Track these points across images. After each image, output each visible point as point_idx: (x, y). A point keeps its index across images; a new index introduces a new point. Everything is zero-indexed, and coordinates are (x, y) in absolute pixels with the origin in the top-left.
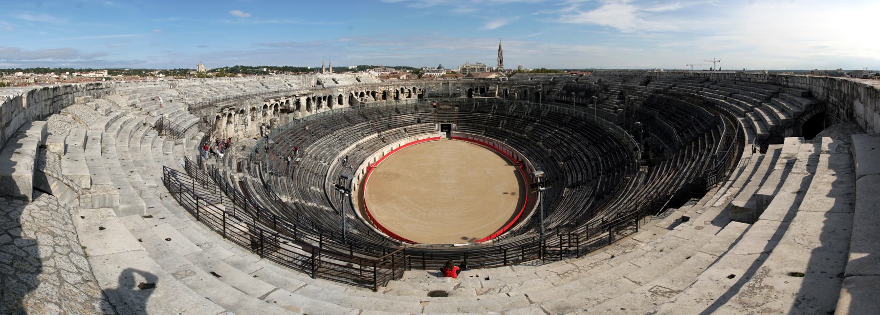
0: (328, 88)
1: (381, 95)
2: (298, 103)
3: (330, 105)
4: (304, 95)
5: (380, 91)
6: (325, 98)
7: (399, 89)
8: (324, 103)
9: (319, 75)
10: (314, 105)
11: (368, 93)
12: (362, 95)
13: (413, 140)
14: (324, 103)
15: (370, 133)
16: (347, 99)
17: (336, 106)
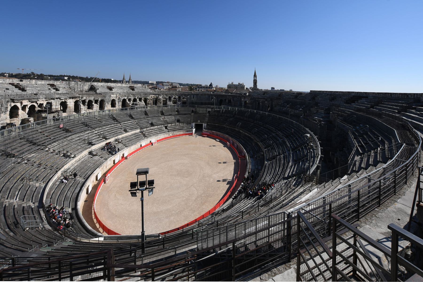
0: (100, 94)
1: (152, 102)
2: (64, 105)
3: (102, 107)
4: (73, 98)
5: (151, 97)
6: (96, 102)
7: (167, 97)
8: (96, 107)
9: (95, 84)
10: (84, 109)
11: (140, 100)
12: (135, 100)
13: (171, 135)
14: (96, 107)
15: (132, 129)
16: (121, 103)
17: (108, 107)
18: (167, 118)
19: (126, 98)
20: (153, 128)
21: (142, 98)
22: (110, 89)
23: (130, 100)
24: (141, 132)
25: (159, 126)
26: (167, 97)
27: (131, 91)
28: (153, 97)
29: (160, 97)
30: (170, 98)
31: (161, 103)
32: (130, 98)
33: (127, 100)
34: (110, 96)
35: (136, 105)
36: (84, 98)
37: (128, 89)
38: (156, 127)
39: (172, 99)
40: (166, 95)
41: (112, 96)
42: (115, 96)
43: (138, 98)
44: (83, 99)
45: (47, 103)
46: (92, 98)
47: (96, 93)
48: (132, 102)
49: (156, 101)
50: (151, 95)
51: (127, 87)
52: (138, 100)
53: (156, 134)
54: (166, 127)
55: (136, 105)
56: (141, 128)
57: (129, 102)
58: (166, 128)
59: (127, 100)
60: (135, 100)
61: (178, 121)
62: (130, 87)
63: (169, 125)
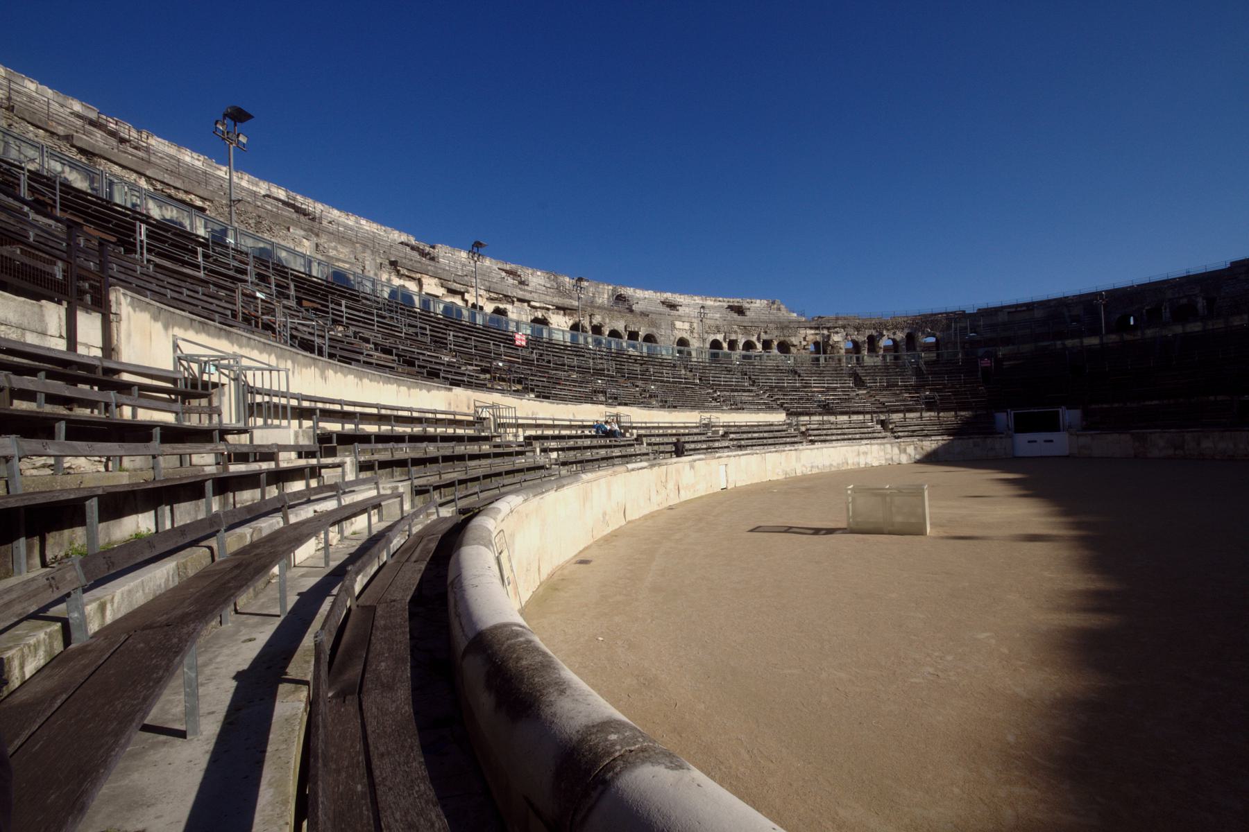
0: (644, 314)
7: (862, 338)
19: (720, 337)
20: (832, 418)
22: (673, 306)
25: (855, 417)
26: (862, 338)
27: (736, 316)
28: (810, 338)
29: (836, 338)
30: (872, 341)
32: (733, 337)
34: (673, 326)
36: (597, 320)
38: (845, 418)
40: (858, 329)
41: (678, 324)
42: (687, 326)
43: (759, 339)
44: (595, 322)
45: (498, 311)
46: (620, 326)
47: (631, 311)
50: (803, 332)
54: (883, 423)
56: (789, 414)
59: (725, 345)
60: (749, 345)
61: (930, 406)
63: (896, 417)
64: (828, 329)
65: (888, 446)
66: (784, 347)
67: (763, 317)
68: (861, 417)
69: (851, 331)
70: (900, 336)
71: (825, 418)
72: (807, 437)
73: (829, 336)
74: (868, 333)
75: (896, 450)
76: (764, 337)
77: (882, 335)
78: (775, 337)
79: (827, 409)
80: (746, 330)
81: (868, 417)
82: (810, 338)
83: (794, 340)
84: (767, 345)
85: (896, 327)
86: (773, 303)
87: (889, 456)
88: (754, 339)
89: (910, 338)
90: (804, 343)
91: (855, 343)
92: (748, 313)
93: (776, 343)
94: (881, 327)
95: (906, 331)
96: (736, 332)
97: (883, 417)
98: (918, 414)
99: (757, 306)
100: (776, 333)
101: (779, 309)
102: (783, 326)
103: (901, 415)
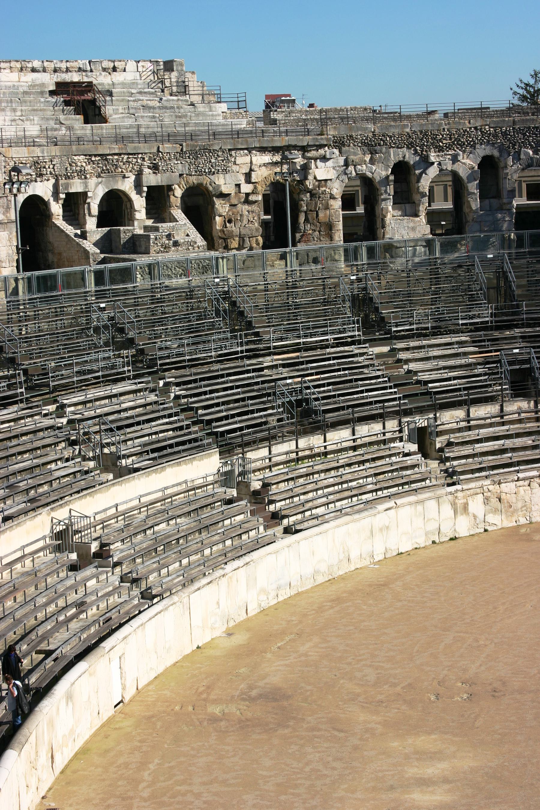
7: (380, 172)
12: (115, 209)
15: (160, 454)
18: (430, 362)
19: (43, 189)
20: (316, 441)
21: (169, 188)
23: (74, 205)
24: (226, 479)
25: (363, 430)
26: (380, 172)
29: (321, 171)
31: (330, 227)
32: (76, 187)
33: (56, 209)
35: (137, 245)
37: (51, 107)
39: (425, 184)
43: (138, 185)
48: (91, 224)
49: (283, 212)
51: (36, 90)
52: (139, 203)
53: (356, 498)
54: (422, 437)
55: (137, 245)
56: (226, 450)
57: (70, 230)
58: (424, 451)
59: (56, 209)
60: (115, 209)
62: (62, 88)
63: (450, 418)
64: (304, 149)
65: (432, 504)
66: (199, 206)
67: (147, 123)
68: (377, 427)
69: (357, 154)
70: (467, 163)
71: (303, 443)
72: (268, 511)
73: (305, 168)
74: (395, 156)
75: (447, 510)
76: (151, 179)
77: (426, 163)
78: (177, 178)
79: (306, 417)
80: (107, 165)
81: (392, 425)
82: (257, 176)
83: (224, 183)
84: (158, 199)
85: (460, 142)
86: (169, 66)
87: (432, 526)
88: (127, 185)
89: (489, 167)
90: (246, 188)
91: (367, 182)
92: (108, 110)
93: (179, 192)
94: (428, 134)
95: (482, 151)
96: (82, 174)
97: (421, 421)
98: (492, 409)
99: (126, 80)
100: (180, 167)
101: (184, 89)
102: (203, 147)
103: (460, 413)
